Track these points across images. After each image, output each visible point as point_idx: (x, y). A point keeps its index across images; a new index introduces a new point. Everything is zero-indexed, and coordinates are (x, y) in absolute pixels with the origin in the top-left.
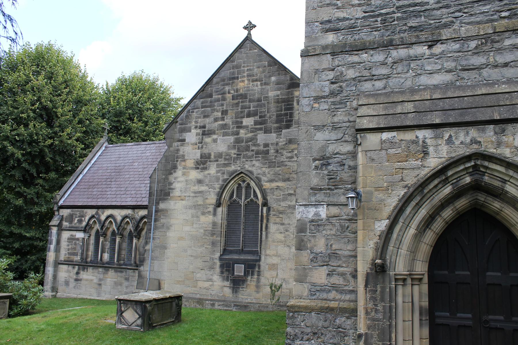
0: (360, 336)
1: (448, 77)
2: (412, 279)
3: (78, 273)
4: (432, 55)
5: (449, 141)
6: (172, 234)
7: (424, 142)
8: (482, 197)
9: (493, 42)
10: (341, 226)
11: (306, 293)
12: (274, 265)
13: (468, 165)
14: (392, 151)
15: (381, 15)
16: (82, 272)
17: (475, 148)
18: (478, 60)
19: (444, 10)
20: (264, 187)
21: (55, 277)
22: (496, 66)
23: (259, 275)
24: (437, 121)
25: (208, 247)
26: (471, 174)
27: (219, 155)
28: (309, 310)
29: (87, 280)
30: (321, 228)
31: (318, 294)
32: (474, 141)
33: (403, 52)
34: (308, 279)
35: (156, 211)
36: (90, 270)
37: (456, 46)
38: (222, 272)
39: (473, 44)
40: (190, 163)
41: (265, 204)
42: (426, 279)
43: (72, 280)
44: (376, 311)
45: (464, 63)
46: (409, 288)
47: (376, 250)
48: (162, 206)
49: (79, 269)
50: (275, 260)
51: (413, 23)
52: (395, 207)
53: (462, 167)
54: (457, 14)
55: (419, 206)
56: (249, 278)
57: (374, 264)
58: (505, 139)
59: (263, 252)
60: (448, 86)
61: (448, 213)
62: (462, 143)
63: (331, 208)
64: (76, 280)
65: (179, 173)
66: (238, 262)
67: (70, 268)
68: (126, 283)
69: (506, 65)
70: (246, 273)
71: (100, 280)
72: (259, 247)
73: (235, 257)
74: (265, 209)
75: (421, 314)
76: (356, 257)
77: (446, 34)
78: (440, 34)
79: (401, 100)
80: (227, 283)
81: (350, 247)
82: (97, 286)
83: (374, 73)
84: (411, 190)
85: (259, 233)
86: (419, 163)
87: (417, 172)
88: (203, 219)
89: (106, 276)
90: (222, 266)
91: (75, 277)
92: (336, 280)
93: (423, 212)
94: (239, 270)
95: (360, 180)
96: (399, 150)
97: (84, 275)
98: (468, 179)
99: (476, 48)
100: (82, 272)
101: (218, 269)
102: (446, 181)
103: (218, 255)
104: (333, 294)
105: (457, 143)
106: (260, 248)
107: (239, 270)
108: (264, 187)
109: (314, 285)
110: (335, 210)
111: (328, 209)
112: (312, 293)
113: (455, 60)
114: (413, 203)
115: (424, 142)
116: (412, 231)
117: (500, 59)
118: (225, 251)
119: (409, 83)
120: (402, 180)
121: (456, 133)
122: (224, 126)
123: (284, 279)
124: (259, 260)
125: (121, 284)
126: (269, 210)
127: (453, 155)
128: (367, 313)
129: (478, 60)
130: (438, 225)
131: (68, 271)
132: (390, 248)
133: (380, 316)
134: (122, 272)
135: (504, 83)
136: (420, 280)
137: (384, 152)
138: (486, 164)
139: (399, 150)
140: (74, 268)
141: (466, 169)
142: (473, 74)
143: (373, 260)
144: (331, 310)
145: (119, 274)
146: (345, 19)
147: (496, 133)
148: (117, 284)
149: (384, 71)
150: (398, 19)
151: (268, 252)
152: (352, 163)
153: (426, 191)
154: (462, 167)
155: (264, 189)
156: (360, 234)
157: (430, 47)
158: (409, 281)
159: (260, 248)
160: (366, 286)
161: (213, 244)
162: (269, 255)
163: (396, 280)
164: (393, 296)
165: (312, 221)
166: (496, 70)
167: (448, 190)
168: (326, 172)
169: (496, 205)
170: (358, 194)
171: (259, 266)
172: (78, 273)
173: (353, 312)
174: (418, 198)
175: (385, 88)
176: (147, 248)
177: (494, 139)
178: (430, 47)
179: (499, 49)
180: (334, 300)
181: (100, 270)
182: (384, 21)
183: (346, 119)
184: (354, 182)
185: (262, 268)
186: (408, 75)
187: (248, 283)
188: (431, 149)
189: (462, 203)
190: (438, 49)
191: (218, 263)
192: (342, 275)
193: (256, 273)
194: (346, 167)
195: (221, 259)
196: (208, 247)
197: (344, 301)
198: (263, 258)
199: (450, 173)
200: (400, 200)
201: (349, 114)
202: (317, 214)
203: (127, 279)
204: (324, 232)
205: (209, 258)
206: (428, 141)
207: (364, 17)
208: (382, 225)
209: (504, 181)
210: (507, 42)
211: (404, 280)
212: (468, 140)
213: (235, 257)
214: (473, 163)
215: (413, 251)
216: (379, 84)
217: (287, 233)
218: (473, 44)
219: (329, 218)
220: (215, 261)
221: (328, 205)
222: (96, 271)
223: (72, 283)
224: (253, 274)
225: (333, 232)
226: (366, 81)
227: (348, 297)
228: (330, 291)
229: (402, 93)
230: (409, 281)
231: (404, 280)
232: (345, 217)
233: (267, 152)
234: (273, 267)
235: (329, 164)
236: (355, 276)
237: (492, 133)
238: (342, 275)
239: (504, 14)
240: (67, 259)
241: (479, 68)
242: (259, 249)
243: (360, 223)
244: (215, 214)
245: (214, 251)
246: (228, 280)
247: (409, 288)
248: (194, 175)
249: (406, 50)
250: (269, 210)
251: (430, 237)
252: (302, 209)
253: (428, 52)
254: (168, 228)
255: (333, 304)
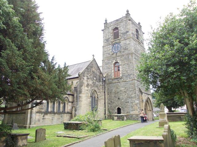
3: (44, 116)
6: (82, 103)
16: (45, 116)
21: (31, 118)
27: (90, 85)
29: (48, 118)
35: (79, 96)
36: (49, 115)
40: (85, 85)
43: (41, 119)
48: (80, 95)
49: (44, 114)
64: (43, 119)
65: (83, 87)
67: (40, 114)
68: (61, 118)
71: (53, 118)
82: (51, 120)
88: (88, 99)
89: (55, 116)
91: (42, 118)
97: (46, 117)
100: (45, 116)
122: (91, 78)
125: (60, 119)
131: (39, 116)
134: (60, 115)
140: (42, 114)
145: (59, 115)
148: (59, 119)
172: (44, 116)
176: (77, 106)
181: (53, 114)
203: (61, 117)
222: (51, 115)
223: (41, 120)
233: (98, 86)
240: (38, 111)
244: (90, 99)
248: (86, 88)
254: (82, 101)
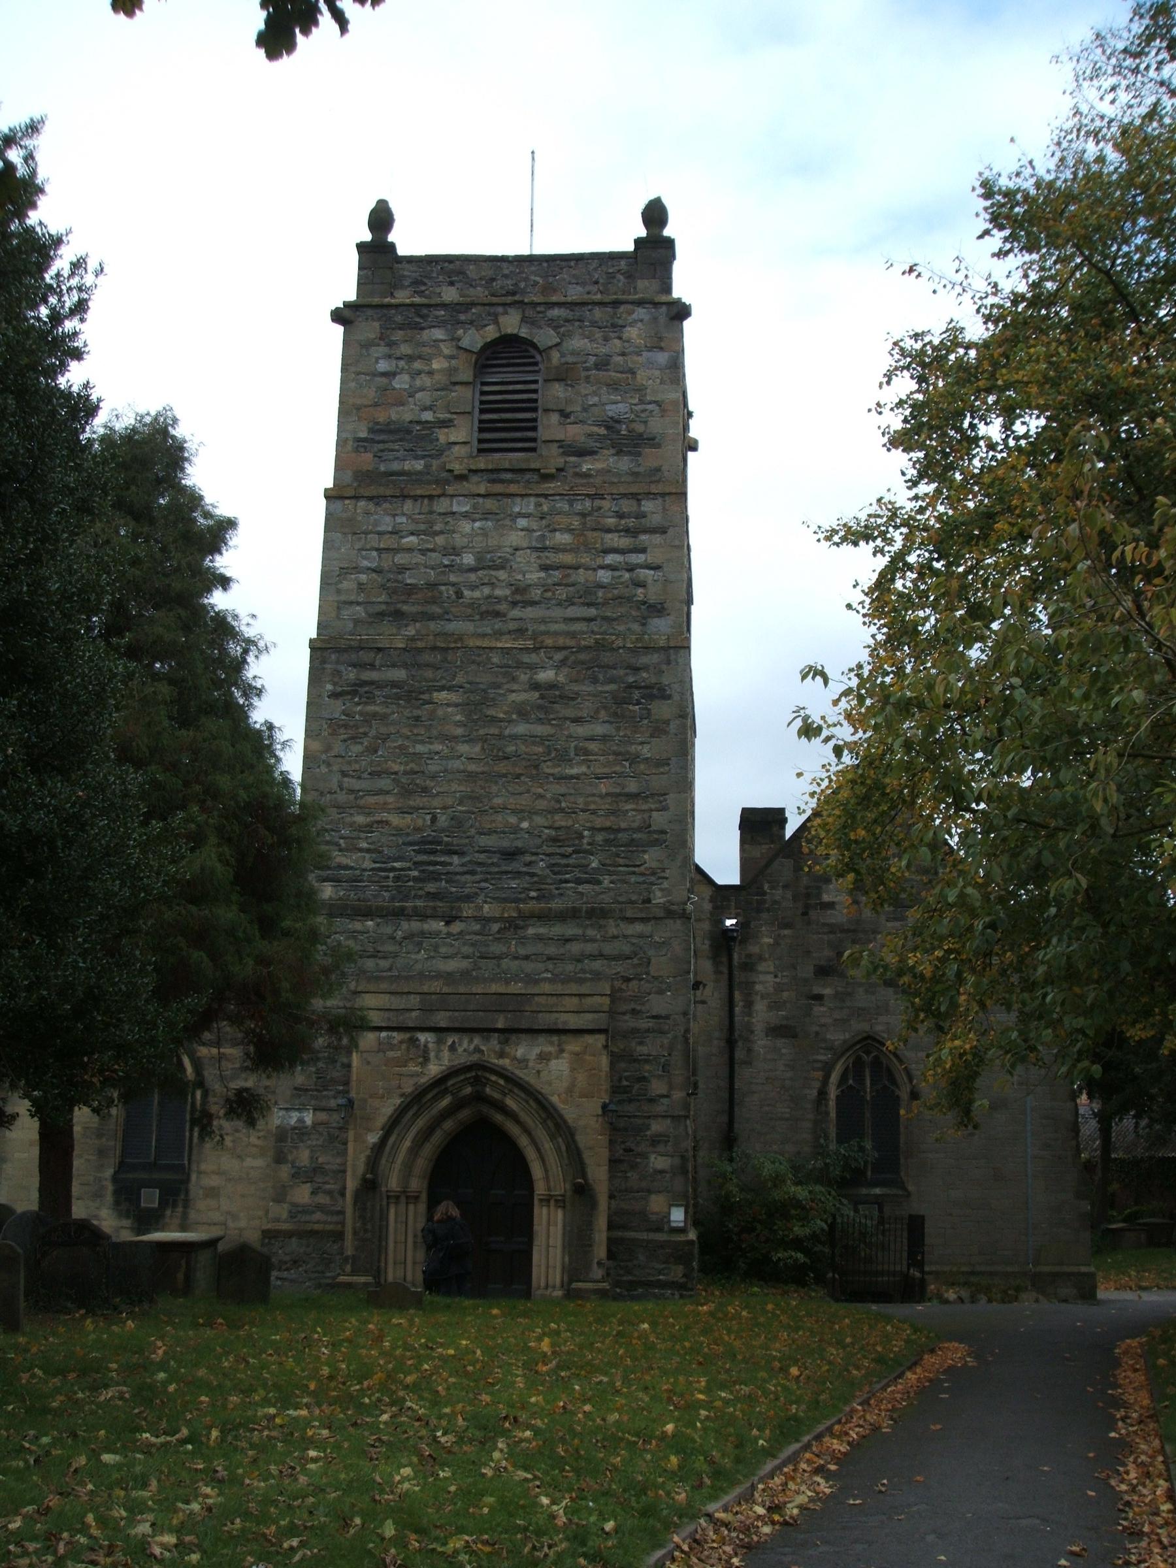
0: (346, 1259)
1: (465, 964)
2: (407, 1197)
4: (449, 934)
5: (452, 1048)
7: (425, 1046)
8: (485, 1109)
9: (517, 927)
10: (329, 1134)
11: (285, 1215)
12: (213, 1188)
13: (468, 1075)
14: (391, 1054)
15: (393, 869)
17: (475, 1058)
18: (497, 948)
19: (468, 877)
20: (199, 1054)
22: (516, 958)
23: (186, 1206)
24: (443, 1024)
25: (91, 1157)
26: (472, 1084)
28: (290, 1234)
30: (306, 1138)
31: (299, 1215)
32: (477, 1050)
33: (415, 925)
34: (288, 1197)
37: (477, 927)
38: (117, 1203)
39: (495, 927)
41: (200, 1083)
42: (424, 1196)
44: (366, 1231)
45: (483, 949)
46: (402, 1207)
47: (367, 1164)
50: (213, 1181)
51: (431, 887)
52: (390, 1117)
53: (462, 1077)
54: (483, 885)
55: (416, 1115)
56: (168, 1212)
57: (364, 1180)
58: (507, 1049)
59: (194, 1167)
60: (465, 975)
61: (448, 1125)
62: (465, 1050)
63: (318, 1113)
66: (149, 1184)
69: (526, 958)
70: (163, 1203)
72: (186, 1158)
73: (143, 1175)
74: (199, 1094)
75: (415, 1236)
76: (344, 1171)
77: (468, 910)
78: (460, 909)
79: (406, 990)
80: (127, 1223)
81: (339, 1160)
83: (380, 948)
84: (409, 1099)
85: (187, 1134)
86: (418, 1069)
87: (415, 1079)
90: (117, 1192)
92: (323, 1199)
93: (421, 1123)
94: (150, 1198)
95: (353, 1084)
96: (399, 1054)
98: (468, 1090)
99: (498, 932)
101: (109, 1198)
102: (445, 1091)
103: (109, 1172)
104: (318, 1216)
105: (460, 1050)
106: (189, 1160)
107: (150, 1198)
108: (199, 1054)
109: (295, 1205)
110: (323, 1116)
111: (314, 1115)
112: (292, 1215)
113: (472, 945)
114: (411, 1113)
115: (425, 1046)
116: (407, 1143)
117: (522, 951)
118: (122, 1166)
119: (418, 967)
120: (399, 1087)
121: (461, 1040)
123: (228, 1213)
124: (188, 1180)
126: (206, 1094)
127: (456, 1063)
128: (355, 1233)
129: (497, 948)
130: (437, 1138)
132: (383, 1161)
133: (369, 1235)
135: (521, 980)
136: (417, 1198)
137: (381, 1055)
138: (488, 1075)
139: (399, 1054)
141: (466, 1079)
142: (492, 964)
143: (364, 1175)
144: (313, 1233)
146: (347, 868)
147: (500, 1043)
149: (390, 947)
150: (415, 879)
151: (203, 1167)
152: (345, 1060)
153: (425, 1100)
154: (462, 1077)
155: (199, 1058)
156: (351, 1146)
157: (448, 923)
158: (403, 1199)
159: (189, 1160)
160: (355, 1203)
161: (101, 1153)
162: (205, 1173)
163: (388, 1197)
164: (384, 1217)
165: (294, 1128)
166: (517, 962)
167: (445, 1102)
168: (314, 1069)
169: (499, 1118)
170: (351, 1102)
171: (187, 1191)
173: (339, 1236)
174: (415, 1108)
175: (390, 969)
177: (497, 1048)
178: (448, 923)
179: (523, 938)
180: (318, 1222)
182: (397, 879)
183: (341, 1004)
184: (347, 1083)
185: (192, 1194)
186: (419, 957)
187: (167, 1220)
188: (432, 1055)
189: (464, 1114)
190: (456, 927)
191: (110, 1188)
192: (329, 1193)
193: (180, 1204)
194: (339, 1064)
195: (115, 1179)
196: (91, 1157)
197: (330, 1223)
198: (194, 1177)
199: (450, 1083)
200: (395, 1110)
201: (346, 998)
202: (301, 1120)
204: (309, 1142)
205: (92, 1178)
206: (430, 1045)
207: (373, 869)
208: (373, 1138)
209: (505, 1095)
210: (531, 931)
211: (398, 1197)
212: (472, 1047)
213: (143, 1175)
214: (474, 1074)
215: (408, 1167)
216: (384, 964)
217: (237, 1135)
218: (495, 927)
219: (315, 1125)
220: (105, 1183)
221: (315, 1110)
224: (175, 1205)
225: (320, 1143)
226: (368, 957)
227: (335, 1218)
228: (313, 1212)
229: (408, 978)
230: (403, 1199)
231: (398, 1197)
232: (335, 1125)
234: (213, 1193)
235: (318, 1059)
236: (342, 1194)
237: (496, 1042)
238: (329, 1193)
239: (533, 894)
241: (499, 958)
242: (186, 1162)
243: (351, 1135)
245: (102, 1166)
246: (128, 1217)
247: (402, 1207)
249: (419, 924)
250: (206, 1094)
251: (429, 1150)
252: (281, 1113)
253: (445, 930)
255: (316, 1227)
